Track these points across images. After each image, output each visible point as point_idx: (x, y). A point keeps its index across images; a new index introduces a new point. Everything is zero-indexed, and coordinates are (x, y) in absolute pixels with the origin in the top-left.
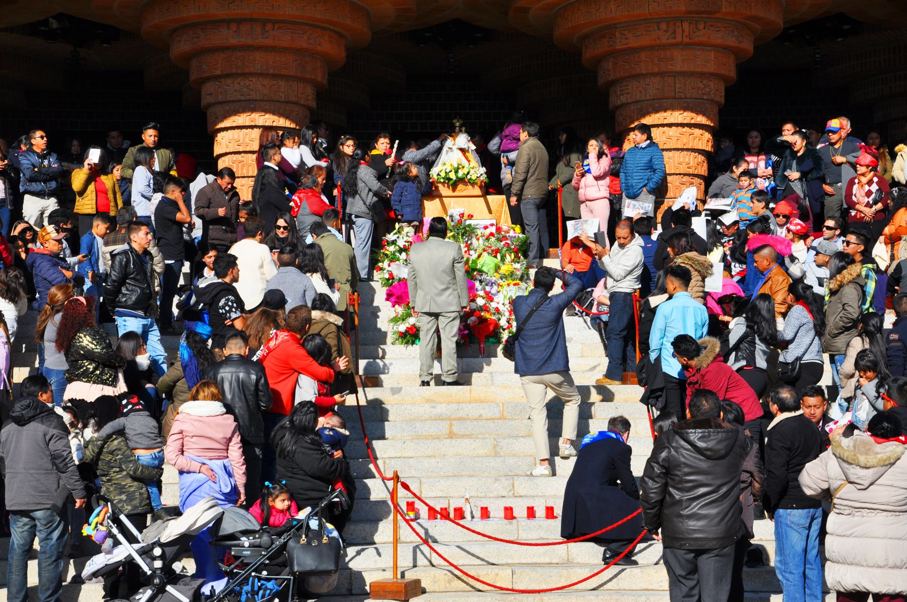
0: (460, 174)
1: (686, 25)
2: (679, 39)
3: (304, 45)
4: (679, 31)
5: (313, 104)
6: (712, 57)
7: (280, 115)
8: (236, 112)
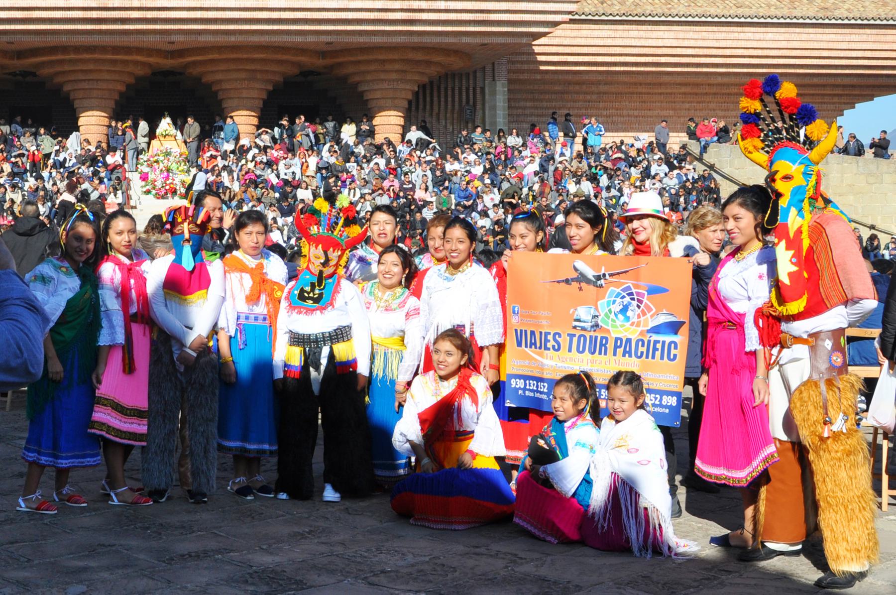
6: (258, 91)
8: (87, 111)
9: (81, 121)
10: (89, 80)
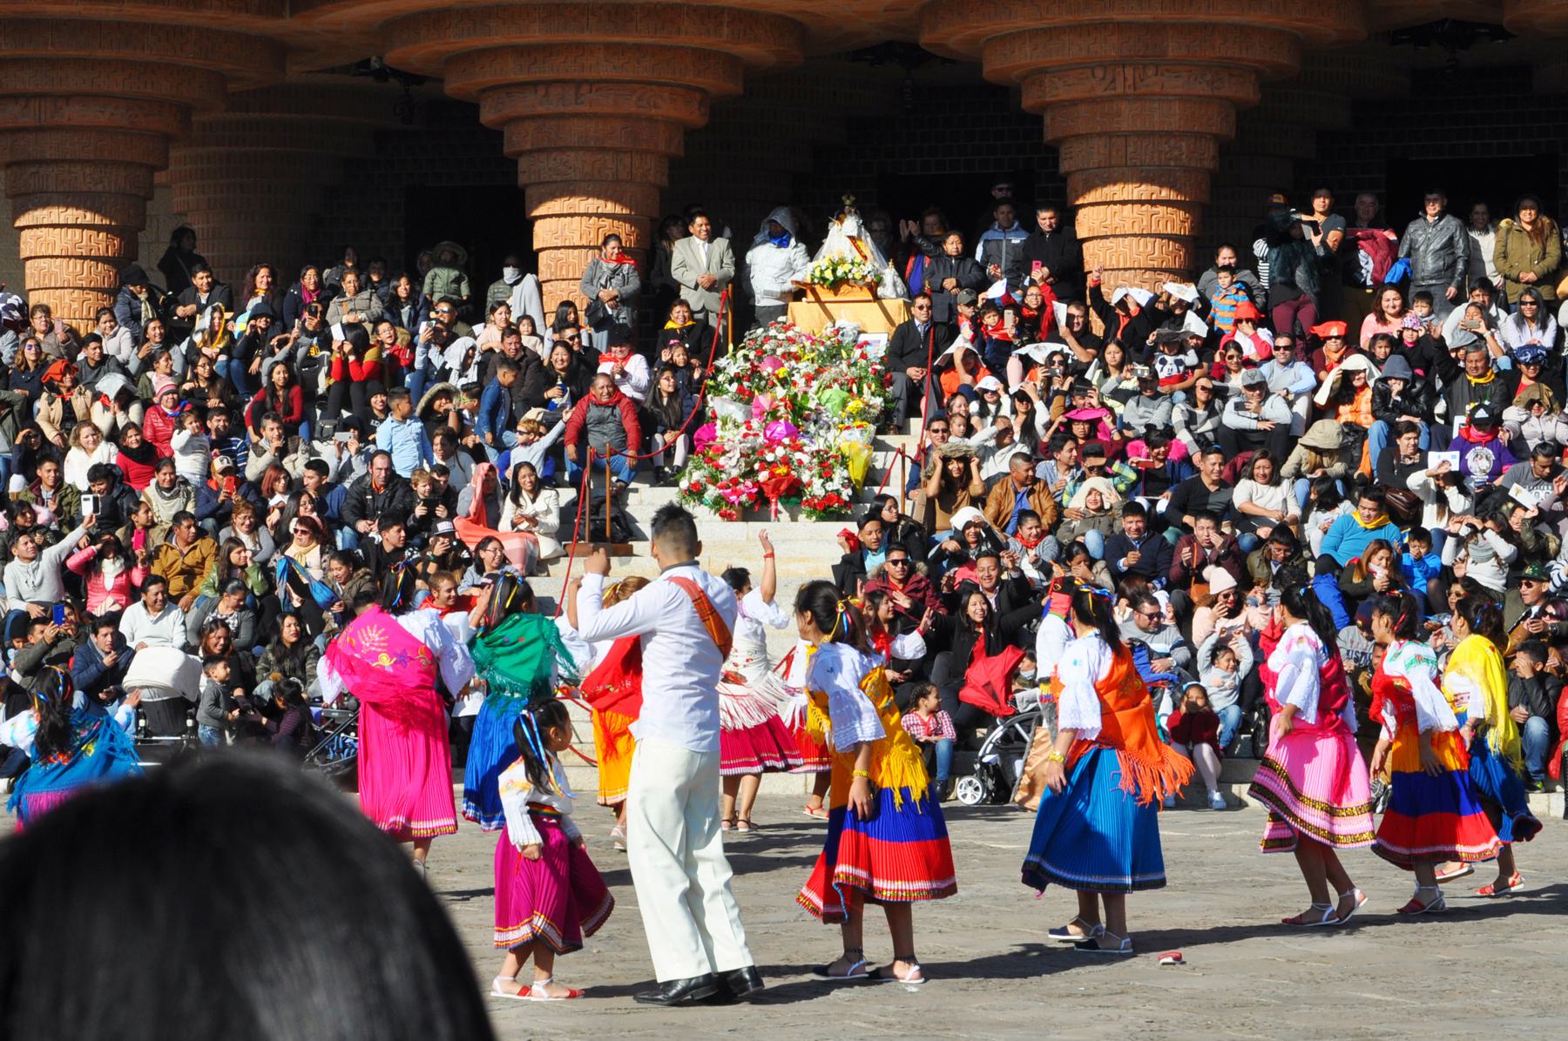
0: (839, 273)
1: (1129, 72)
2: (1120, 90)
3: (633, 109)
4: (1120, 80)
5: (665, 181)
7: (607, 198)
9: (542, 234)
10: (548, 83)
